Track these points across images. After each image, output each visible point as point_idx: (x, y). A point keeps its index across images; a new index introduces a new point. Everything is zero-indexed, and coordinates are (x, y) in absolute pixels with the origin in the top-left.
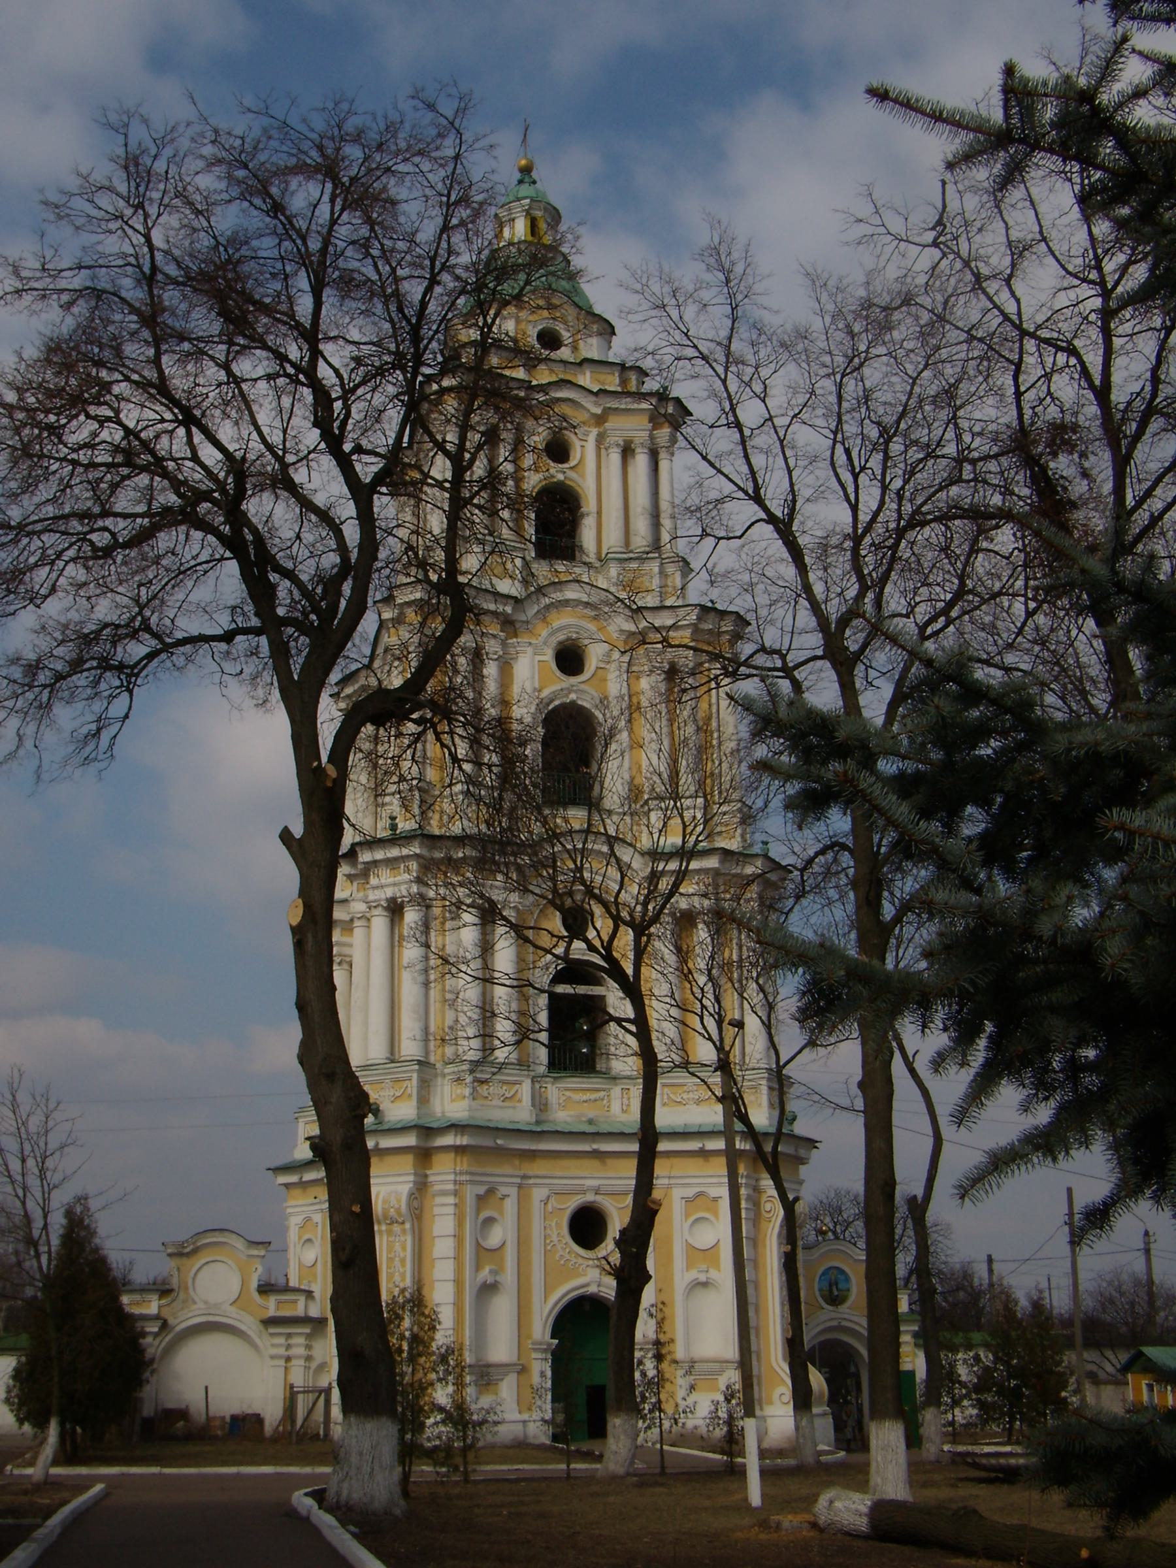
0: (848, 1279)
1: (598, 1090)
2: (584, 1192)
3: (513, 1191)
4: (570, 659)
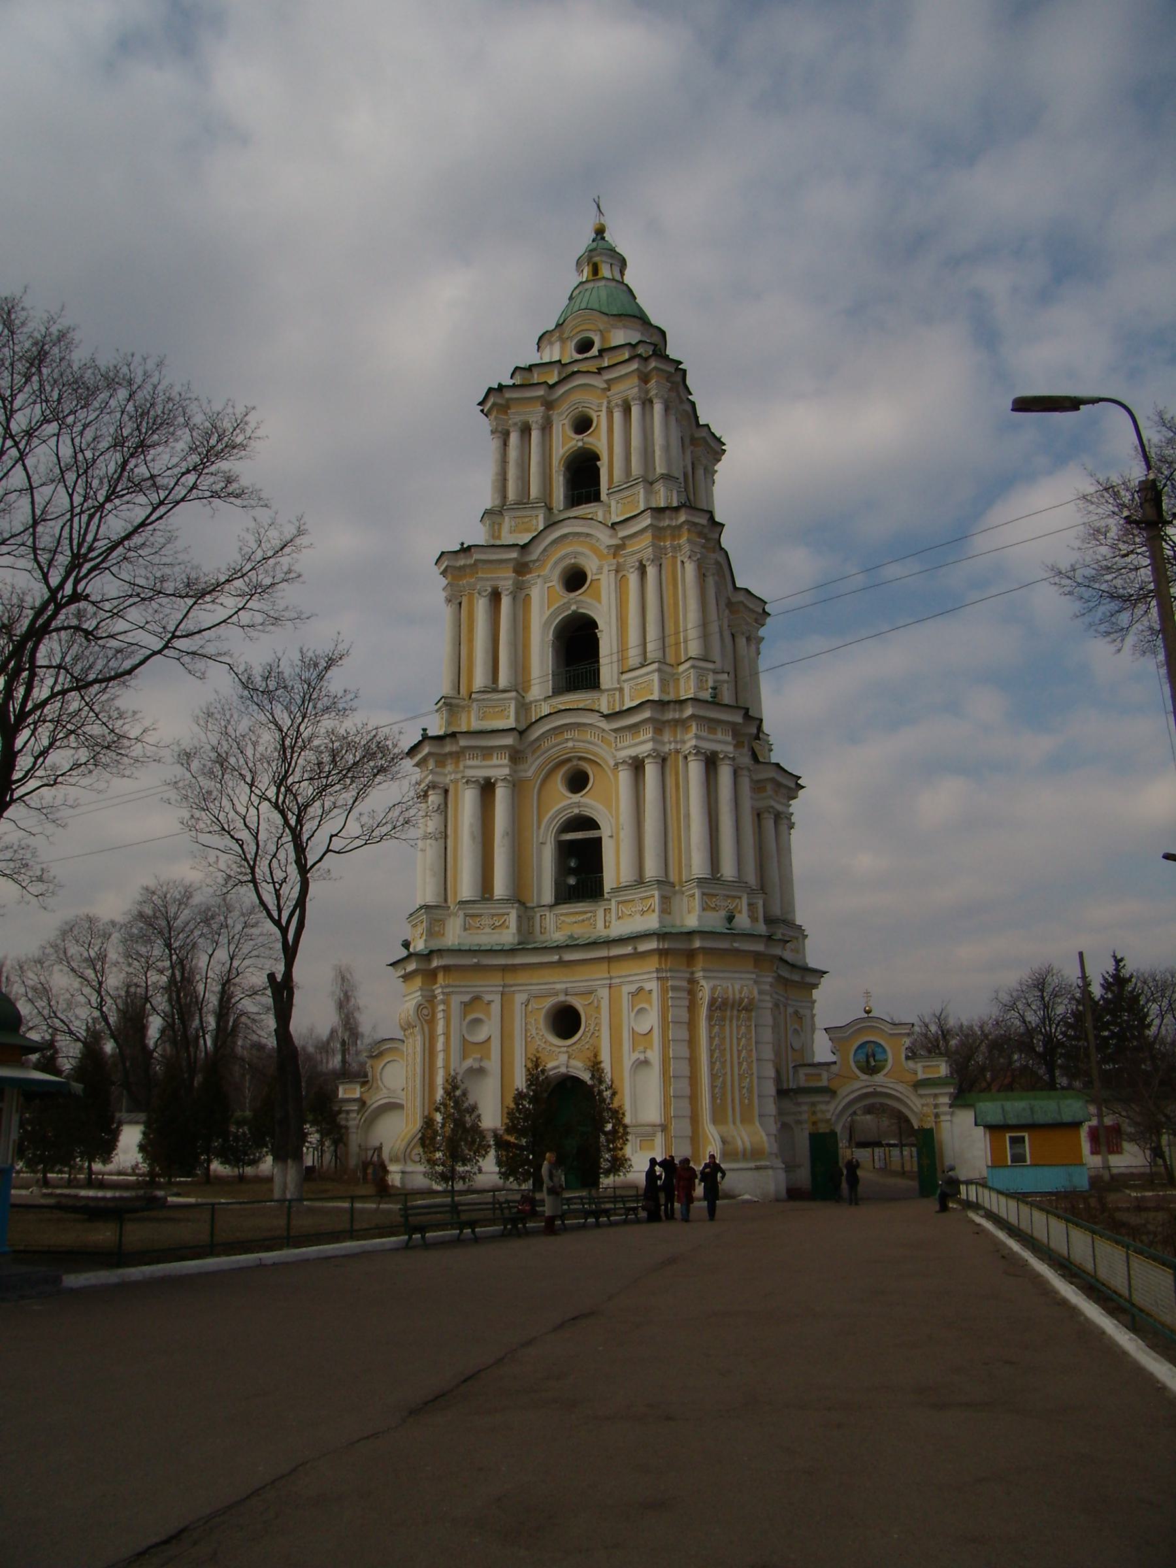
0: (885, 1051)
1: (586, 913)
2: (556, 994)
3: (497, 998)
4: (575, 579)
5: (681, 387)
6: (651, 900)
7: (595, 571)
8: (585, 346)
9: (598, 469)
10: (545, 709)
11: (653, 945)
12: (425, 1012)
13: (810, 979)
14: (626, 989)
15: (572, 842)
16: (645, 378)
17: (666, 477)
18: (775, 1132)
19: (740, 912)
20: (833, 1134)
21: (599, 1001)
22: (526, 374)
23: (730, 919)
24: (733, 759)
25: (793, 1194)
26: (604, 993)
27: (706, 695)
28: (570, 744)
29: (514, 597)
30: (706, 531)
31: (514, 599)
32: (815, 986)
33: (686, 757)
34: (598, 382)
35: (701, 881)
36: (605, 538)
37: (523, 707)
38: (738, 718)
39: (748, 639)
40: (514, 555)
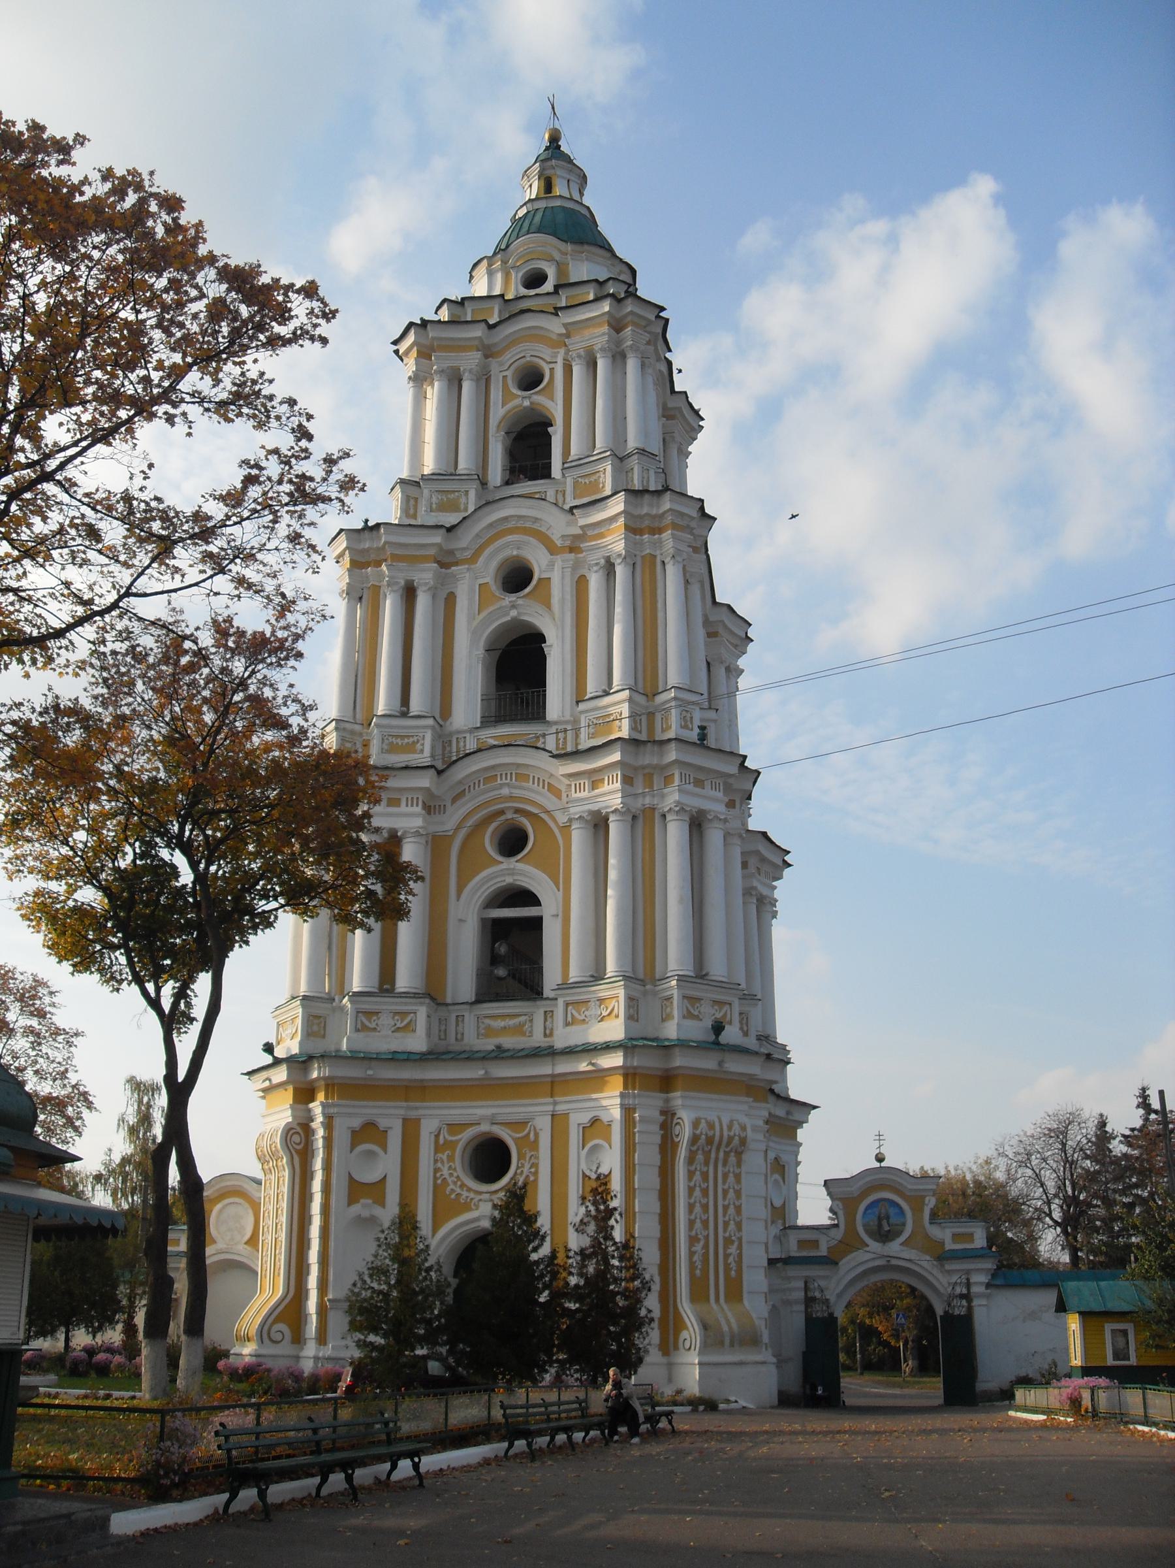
0: (902, 1212)
4: (517, 578)
5: (661, 341)
6: (614, 1001)
7: (543, 567)
8: (535, 280)
9: (549, 437)
10: (471, 745)
11: (616, 1060)
12: (296, 1138)
13: (797, 1116)
14: (579, 1118)
15: (497, 922)
16: (617, 326)
17: (642, 452)
18: (766, 1315)
19: (730, 1023)
20: (832, 1319)
21: (537, 1135)
22: (458, 310)
23: (718, 1028)
24: (726, 821)
25: (785, 1400)
26: (543, 1124)
27: (693, 735)
28: (505, 791)
29: (434, 592)
30: (693, 524)
31: (434, 597)
32: (800, 1124)
33: (664, 816)
34: (555, 326)
35: (681, 979)
36: (558, 526)
37: (443, 738)
38: (733, 769)
39: (728, 669)
40: (437, 538)
